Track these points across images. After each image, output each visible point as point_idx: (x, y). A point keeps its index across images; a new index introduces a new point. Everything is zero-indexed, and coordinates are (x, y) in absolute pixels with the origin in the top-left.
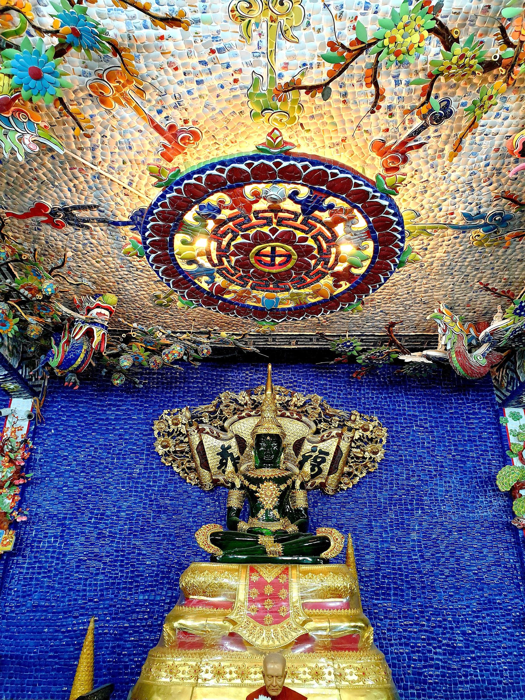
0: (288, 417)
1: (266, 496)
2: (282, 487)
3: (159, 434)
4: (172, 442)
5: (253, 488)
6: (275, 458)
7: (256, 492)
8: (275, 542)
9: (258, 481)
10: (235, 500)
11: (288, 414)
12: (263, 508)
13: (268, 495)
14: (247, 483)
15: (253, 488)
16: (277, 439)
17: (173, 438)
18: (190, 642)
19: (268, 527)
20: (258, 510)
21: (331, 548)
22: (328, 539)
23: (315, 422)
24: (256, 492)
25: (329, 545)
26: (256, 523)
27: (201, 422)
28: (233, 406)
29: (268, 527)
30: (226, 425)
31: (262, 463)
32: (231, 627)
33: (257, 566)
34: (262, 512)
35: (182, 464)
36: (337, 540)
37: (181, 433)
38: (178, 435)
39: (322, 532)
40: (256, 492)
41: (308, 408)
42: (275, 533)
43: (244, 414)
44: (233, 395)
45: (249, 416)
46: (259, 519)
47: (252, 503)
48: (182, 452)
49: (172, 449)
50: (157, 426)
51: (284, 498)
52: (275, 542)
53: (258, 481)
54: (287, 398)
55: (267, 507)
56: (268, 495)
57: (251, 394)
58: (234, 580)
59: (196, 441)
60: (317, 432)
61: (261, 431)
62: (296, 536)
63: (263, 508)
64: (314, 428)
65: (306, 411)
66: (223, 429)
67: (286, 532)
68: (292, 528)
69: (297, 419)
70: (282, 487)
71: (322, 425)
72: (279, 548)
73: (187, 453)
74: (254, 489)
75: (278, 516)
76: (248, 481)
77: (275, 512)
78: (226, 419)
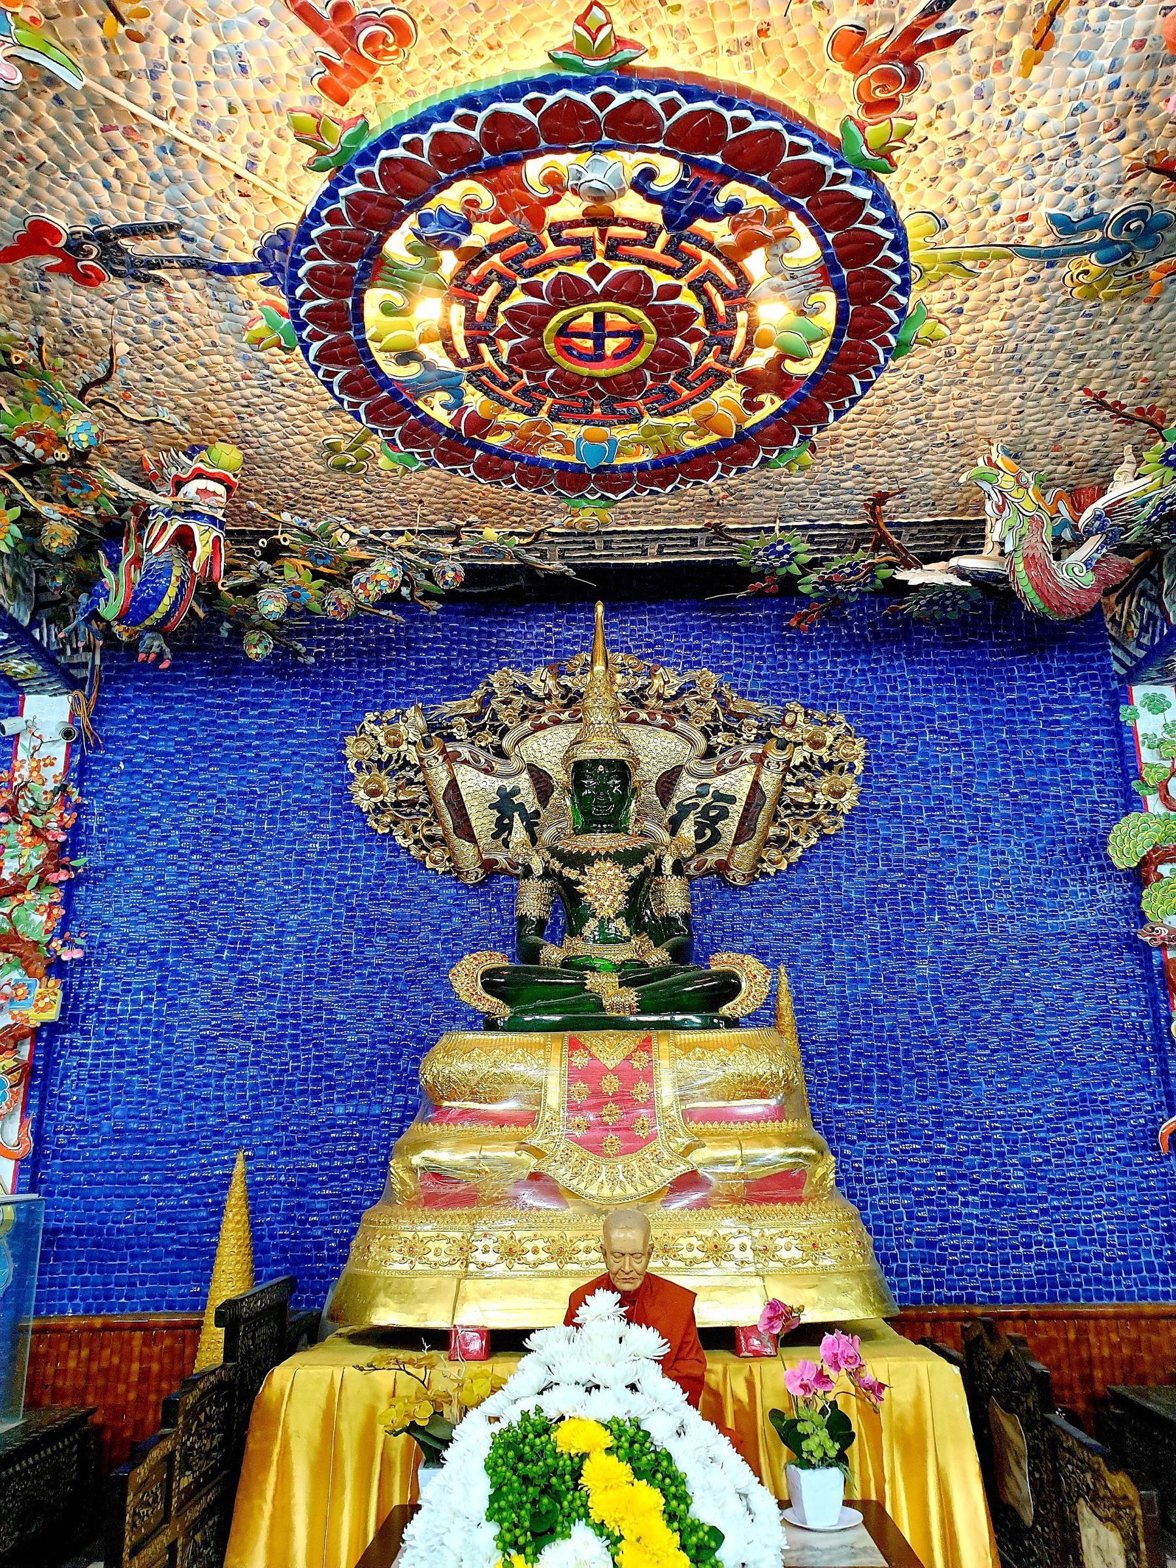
0: (644, 722)
1: (599, 890)
2: (634, 872)
3: (358, 765)
4: (387, 783)
5: (572, 874)
6: (618, 812)
7: (578, 883)
9: (581, 861)
10: (532, 901)
11: (643, 715)
12: (594, 916)
13: (604, 887)
14: (556, 865)
15: (572, 874)
16: (621, 770)
17: (391, 774)
18: (445, 1192)
19: (606, 956)
20: (583, 921)
21: (742, 995)
22: (736, 977)
23: (703, 731)
25: (737, 989)
26: (577, 947)
27: (451, 738)
28: (520, 701)
29: (606, 956)
30: (506, 743)
31: (590, 823)
32: (533, 1162)
33: (585, 1036)
34: (592, 923)
35: (415, 830)
36: (754, 979)
37: (407, 763)
38: (402, 768)
39: (721, 962)
40: (578, 883)
41: (688, 701)
42: (619, 967)
43: (544, 719)
44: (519, 677)
45: (558, 722)
46: (585, 939)
47: (569, 905)
48: (412, 804)
49: (390, 798)
50: (354, 749)
51: (638, 895)
53: (581, 861)
54: (640, 682)
55: (601, 913)
56: (604, 887)
58: (535, 1067)
59: (440, 776)
60: (710, 753)
61: (586, 754)
62: (667, 973)
63: (594, 916)
64: (702, 744)
65: (684, 708)
66: (500, 753)
67: (643, 965)
68: (658, 956)
69: (664, 727)
70: (634, 872)
71: (721, 738)
72: (631, 996)
73: (423, 805)
74: (573, 877)
75: (626, 933)
77: (620, 926)
78: (506, 730)
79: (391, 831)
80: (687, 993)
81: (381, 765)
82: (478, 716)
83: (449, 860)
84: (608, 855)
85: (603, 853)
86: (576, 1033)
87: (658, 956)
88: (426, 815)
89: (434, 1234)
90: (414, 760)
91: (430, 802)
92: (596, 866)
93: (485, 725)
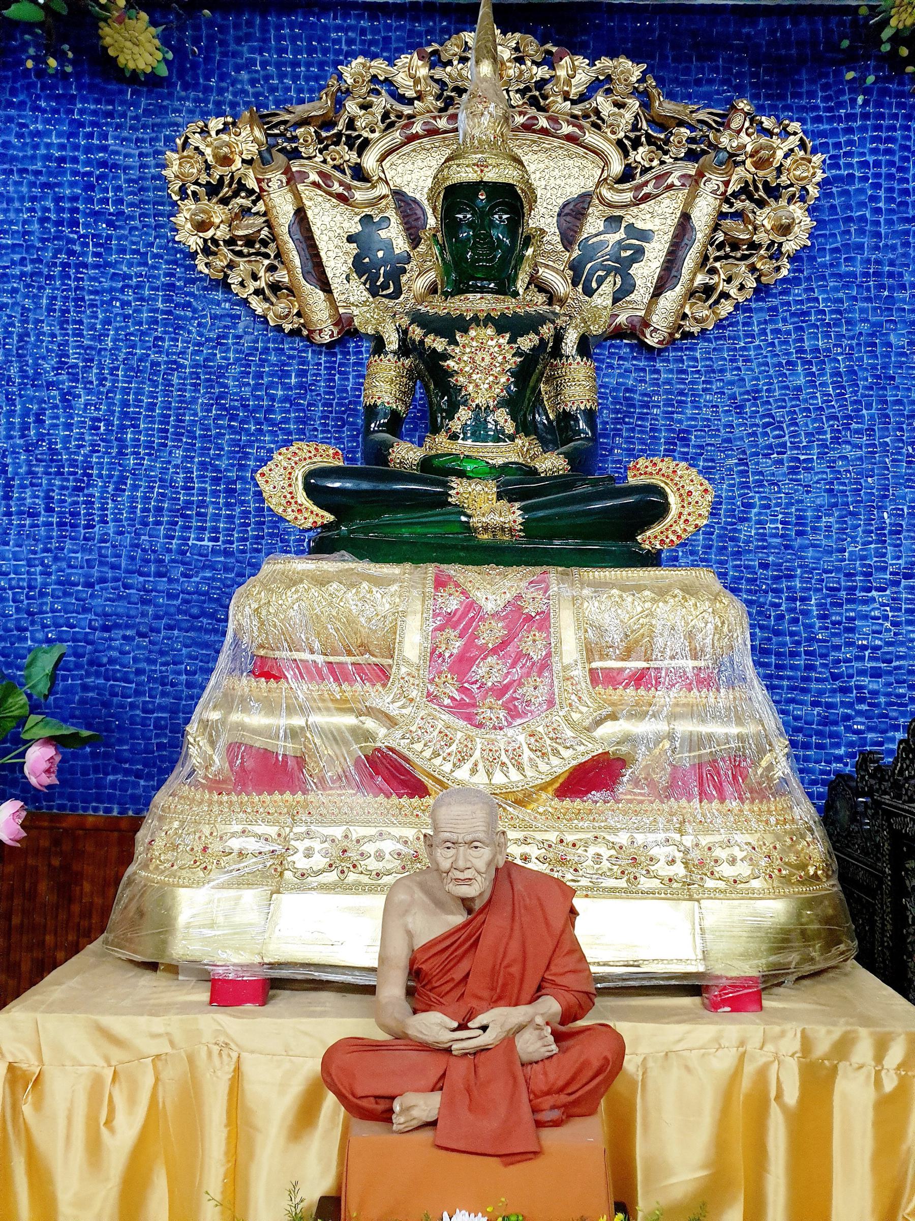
0: (544, 131)
2: (527, 343)
3: (183, 191)
4: (219, 213)
5: (439, 344)
8: (499, 497)
9: (450, 327)
10: (384, 384)
11: (543, 122)
12: (465, 403)
14: (416, 332)
15: (439, 344)
16: (511, 200)
17: (225, 201)
18: (270, 772)
21: (669, 520)
22: (664, 495)
23: (620, 143)
24: (445, 356)
25: (662, 509)
27: (295, 154)
28: (382, 102)
30: (370, 161)
32: (382, 732)
33: (452, 570)
34: (464, 415)
35: (255, 277)
36: (688, 498)
37: (242, 187)
38: (236, 194)
40: (445, 356)
41: (602, 102)
43: (417, 128)
44: (379, 67)
45: (432, 132)
48: (249, 241)
49: (222, 233)
50: (175, 166)
51: (532, 372)
52: (499, 497)
53: (450, 327)
54: (542, 72)
57: (436, 60)
59: (283, 207)
60: (627, 175)
61: (465, 174)
64: (617, 167)
65: (597, 112)
66: (359, 173)
69: (570, 138)
70: (527, 343)
71: (641, 155)
72: (512, 515)
73: (264, 243)
74: (440, 349)
76: (422, 325)
77: (503, 419)
78: (366, 143)
79: (226, 276)
80: (591, 520)
81: (213, 190)
82: (328, 124)
83: (299, 314)
84: (489, 320)
85: (482, 315)
86: (444, 567)
87: (551, 463)
88: (267, 256)
89: (248, 828)
90: (251, 183)
91: (274, 240)
92: (472, 333)
93: (339, 135)
